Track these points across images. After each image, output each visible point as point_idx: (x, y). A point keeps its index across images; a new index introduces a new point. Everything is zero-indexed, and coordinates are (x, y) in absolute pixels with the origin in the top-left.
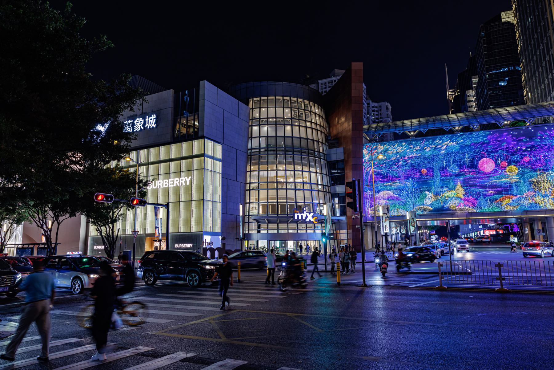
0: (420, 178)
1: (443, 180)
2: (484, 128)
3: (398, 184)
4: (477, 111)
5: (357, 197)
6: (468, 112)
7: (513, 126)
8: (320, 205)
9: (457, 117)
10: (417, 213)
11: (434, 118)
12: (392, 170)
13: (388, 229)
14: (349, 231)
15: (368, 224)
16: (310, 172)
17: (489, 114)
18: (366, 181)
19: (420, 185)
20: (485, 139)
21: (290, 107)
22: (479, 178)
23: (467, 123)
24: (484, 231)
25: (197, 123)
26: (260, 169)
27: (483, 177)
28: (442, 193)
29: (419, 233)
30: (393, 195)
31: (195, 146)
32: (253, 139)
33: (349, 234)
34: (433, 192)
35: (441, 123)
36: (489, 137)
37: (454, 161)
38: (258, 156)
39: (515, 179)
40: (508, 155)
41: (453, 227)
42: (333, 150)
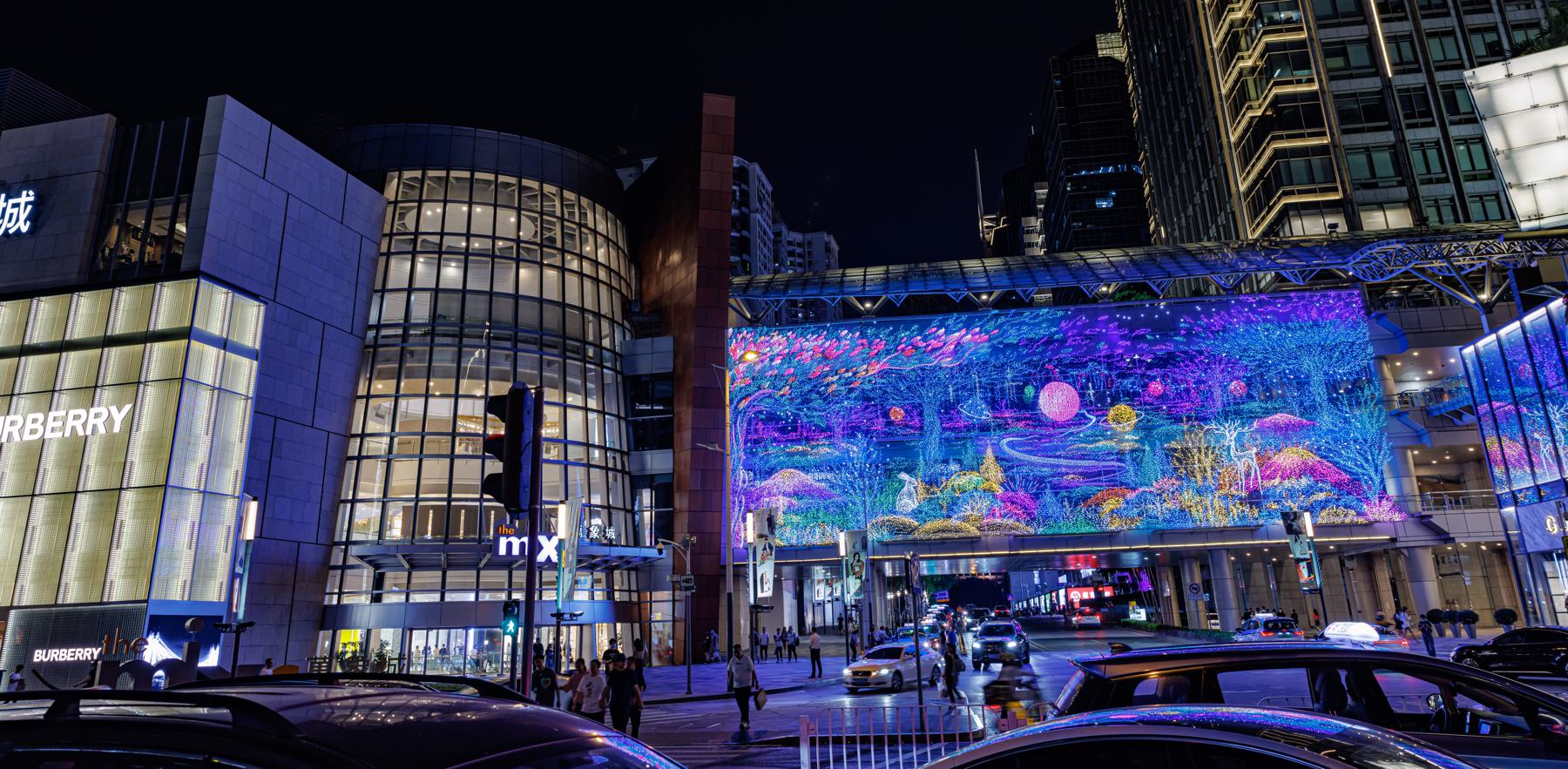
1: (947, 440)
3: (824, 450)
12: (808, 409)
16: (565, 406)
17: (1064, 264)
19: (886, 452)
21: (516, 205)
25: (181, 228)
26: (401, 392)
28: (944, 478)
31: (163, 302)
32: (387, 296)
34: (920, 474)
36: (1063, 324)
38: (399, 348)
39: (1130, 441)
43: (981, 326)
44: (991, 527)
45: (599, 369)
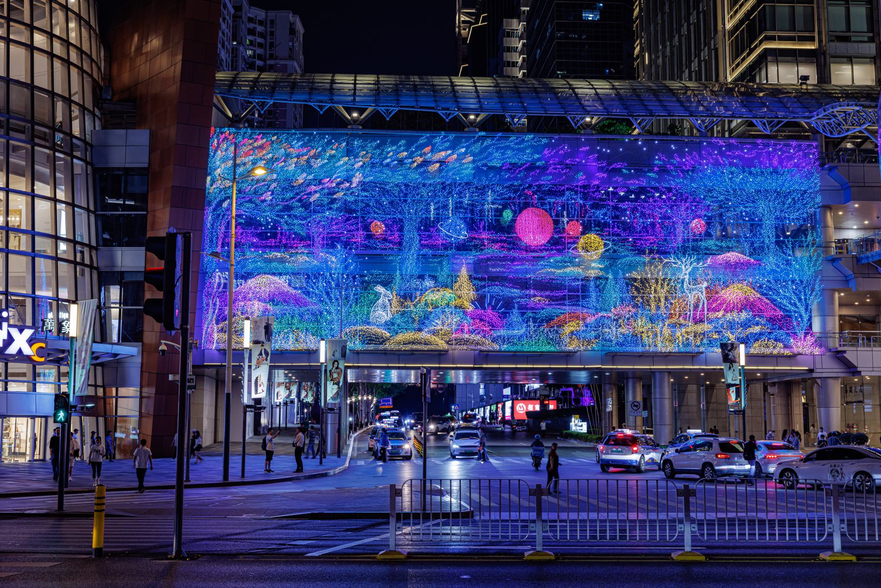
0: (366, 247)
1: (424, 256)
2: (537, 125)
4: (525, 79)
5: (179, 284)
6: (504, 76)
7: (604, 132)
8: (59, 304)
9: (476, 86)
10: (350, 345)
11: (416, 79)
12: (289, 216)
13: (265, 389)
14: (145, 390)
15: (207, 371)
17: (552, 91)
18: (212, 241)
20: (537, 156)
22: (513, 260)
23: (499, 106)
24: (513, 403)
27: (524, 259)
28: (418, 293)
29: (348, 402)
30: (287, 288)
33: (144, 400)
35: (435, 96)
36: (546, 152)
37: (456, 208)
39: (595, 269)
40: (585, 205)
41: (440, 389)
42: (117, 135)
43: (467, 147)
44: (459, 341)
45: (69, 158)
